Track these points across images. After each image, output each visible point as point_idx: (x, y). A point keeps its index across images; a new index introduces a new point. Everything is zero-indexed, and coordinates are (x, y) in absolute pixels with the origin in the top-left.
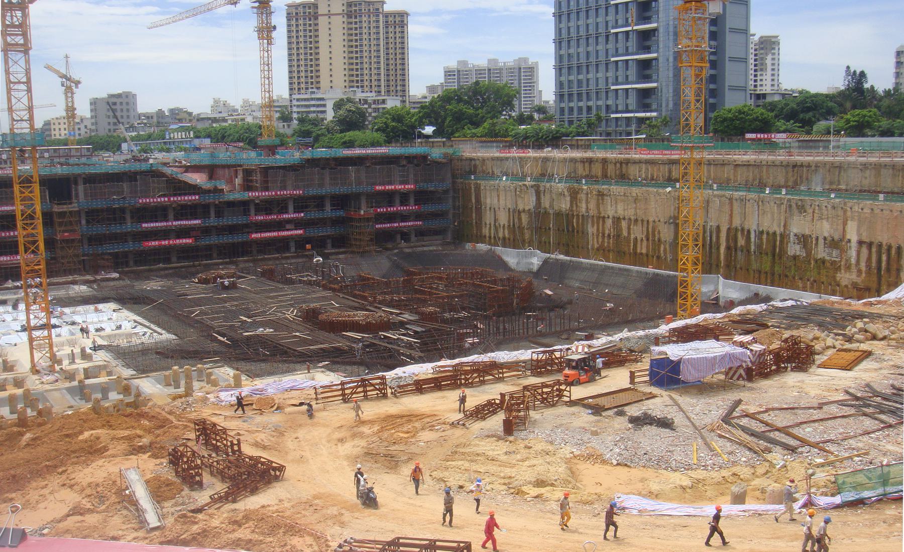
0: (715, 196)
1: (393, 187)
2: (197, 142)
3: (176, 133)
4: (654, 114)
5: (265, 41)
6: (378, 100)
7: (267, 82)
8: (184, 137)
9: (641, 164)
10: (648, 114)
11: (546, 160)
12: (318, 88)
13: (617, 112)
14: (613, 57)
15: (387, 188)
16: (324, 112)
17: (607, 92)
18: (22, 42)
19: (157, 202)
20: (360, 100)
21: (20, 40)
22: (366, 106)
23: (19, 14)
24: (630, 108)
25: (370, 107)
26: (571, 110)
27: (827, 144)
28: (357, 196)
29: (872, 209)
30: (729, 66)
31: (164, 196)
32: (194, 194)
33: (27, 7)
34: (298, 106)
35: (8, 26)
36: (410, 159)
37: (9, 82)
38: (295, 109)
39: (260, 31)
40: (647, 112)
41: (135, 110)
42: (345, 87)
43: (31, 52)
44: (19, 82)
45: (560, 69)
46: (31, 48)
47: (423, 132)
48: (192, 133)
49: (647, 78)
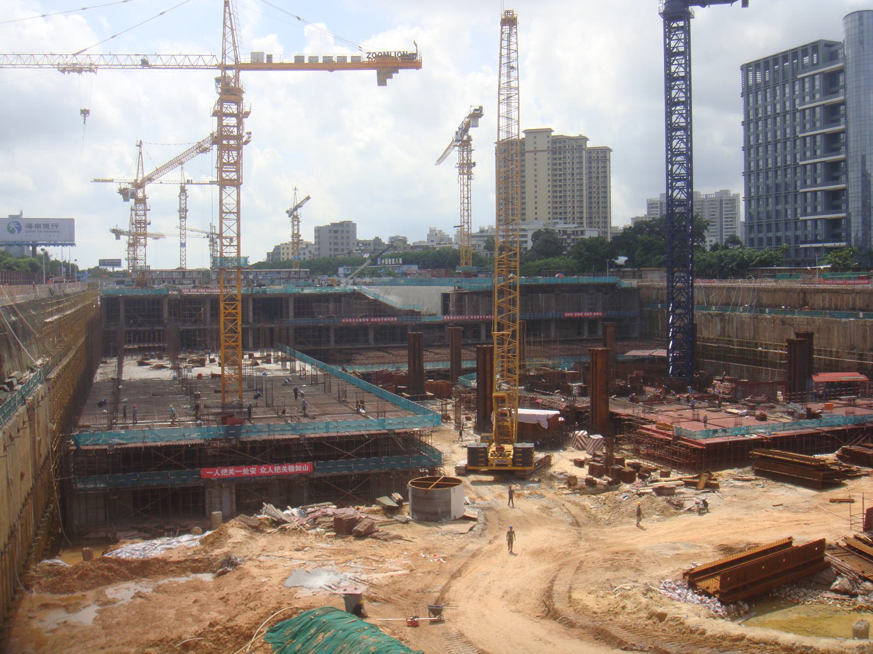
1: (582, 314)
2: (405, 268)
4: (843, 244)
5: (466, 177)
6: (577, 231)
7: (466, 214)
8: (393, 263)
9: (824, 294)
10: (837, 244)
11: (729, 289)
12: (524, 220)
13: (805, 242)
15: (576, 314)
16: (526, 242)
18: (235, 177)
19: (359, 322)
20: (559, 231)
21: (234, 176)
22: (565, 237)
23: (235, 153)
25: (569, 238)
28: (548, 321)
31: (365, 317)
32: (393, 316)
33: (241, 148)
35: (225, 164)
36: (599, 287)
37: (221, 212)
39: (461, 166)
40: (837, 242)
42: (549, 218)
44: (230, 212)
46: (242, 183)
47: (616, 261)
48: (401, 259)
49: (836, 208)
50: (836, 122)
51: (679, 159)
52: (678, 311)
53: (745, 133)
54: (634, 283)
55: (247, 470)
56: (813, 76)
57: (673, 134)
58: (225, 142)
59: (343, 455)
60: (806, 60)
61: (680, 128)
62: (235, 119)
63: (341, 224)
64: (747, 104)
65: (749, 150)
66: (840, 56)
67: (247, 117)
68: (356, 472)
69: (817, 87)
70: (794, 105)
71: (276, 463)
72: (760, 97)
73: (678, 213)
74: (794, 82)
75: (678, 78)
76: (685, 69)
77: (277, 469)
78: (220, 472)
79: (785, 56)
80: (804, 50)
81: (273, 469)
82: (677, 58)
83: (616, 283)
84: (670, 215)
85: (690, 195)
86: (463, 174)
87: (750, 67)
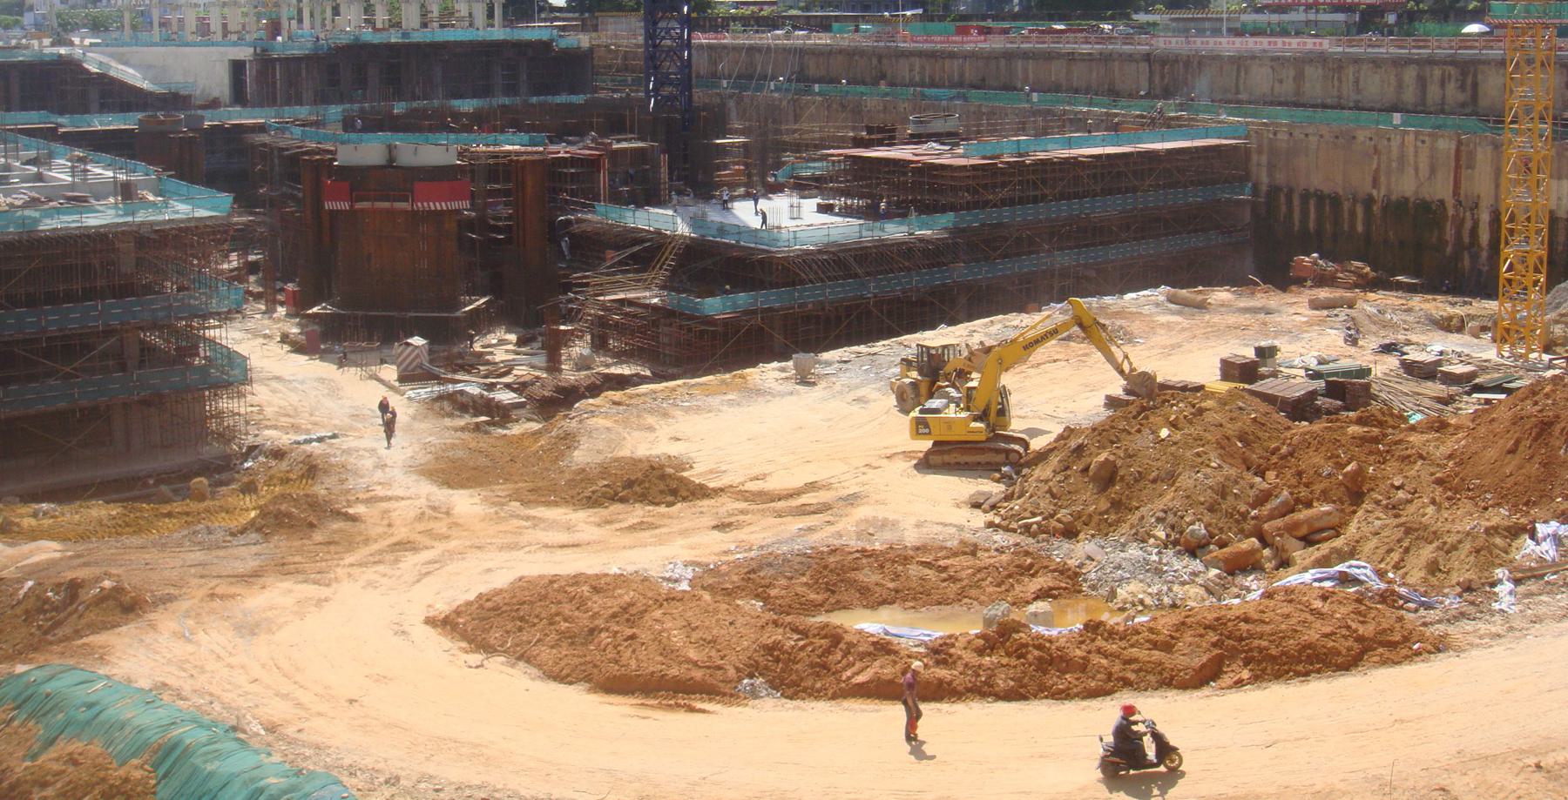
0: (1035, 113)
9: (913, 59)
11: (751, 50)
27: (1218, 25)
29: (1291, 134)
52: (667, 91)
54: (584, 40)
68: (84, 403)
83: (552, 40)
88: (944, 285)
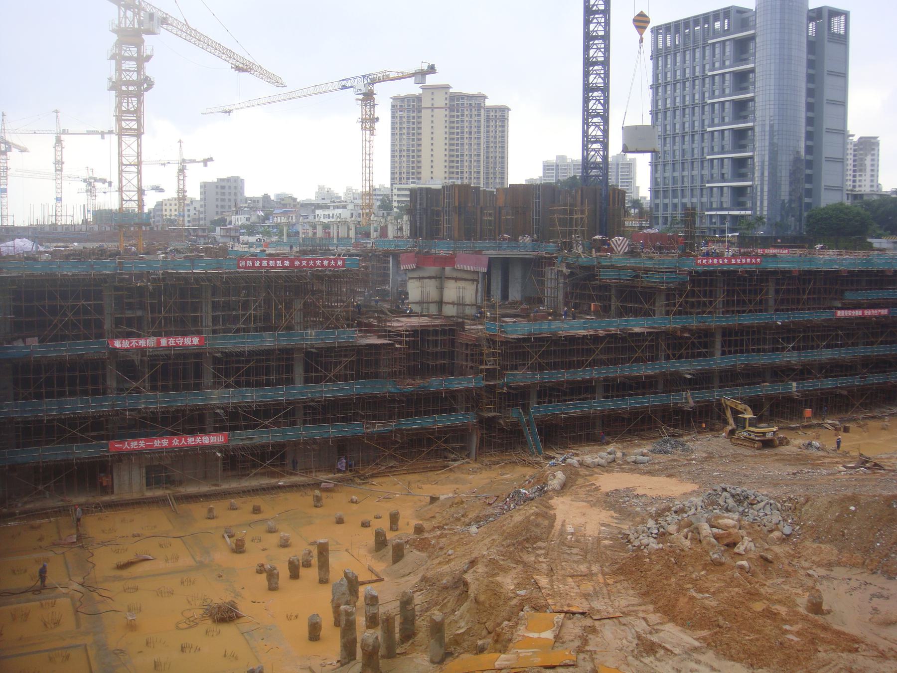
3: (279, 218)
4: (749, 212)
5: (368, 132)
10: (743, 213)
13: (711, 209)
14: (708, 155)
17: (702, 189)
18: (135, 127)
21: (134, 125)
24: (725, 206)
26: (666, 206)
30: (826, 168)
33: (143, 95)
34: (399, 195)
35: (124, 112)
37: (121, 164)
38: (395, 198)
39: (363, 121)
41: (242, 193)
42: (445, 178)
43: (143, 136)
44: (130, 165)
45: (656, 166)
46: (143, 133)
49: (742, 176)
50: (744, 90)
51: (595, 120)
53: (653, 97)
55: (159, 442)
56: (724, 42)
57: (590, 94)
58: (124, 88)
59: (261, 424)
60: (717, 25)
61: (597, 89)
62: (134, 63)
63: (228, 180)
64: (656, 67)
65: (657, 114)
66: (751, 24)
67: (148, 61)
69: (727, 54)
70: (704, 70)
71: (189, 433)
72: (669, 61)
73: (593, 176)
74: (704, 48)
75: (597, 37)
76: (605, 28)
77: (191, 440)
78: (129, 445)
79: (696, 20)
80: (716, 15)
81: (186, 441)
82: (597, 16)
84: (586, 177)
85: (605, 158)
86: (366, 129)
87: (661, 29)
88: (758, 396)
